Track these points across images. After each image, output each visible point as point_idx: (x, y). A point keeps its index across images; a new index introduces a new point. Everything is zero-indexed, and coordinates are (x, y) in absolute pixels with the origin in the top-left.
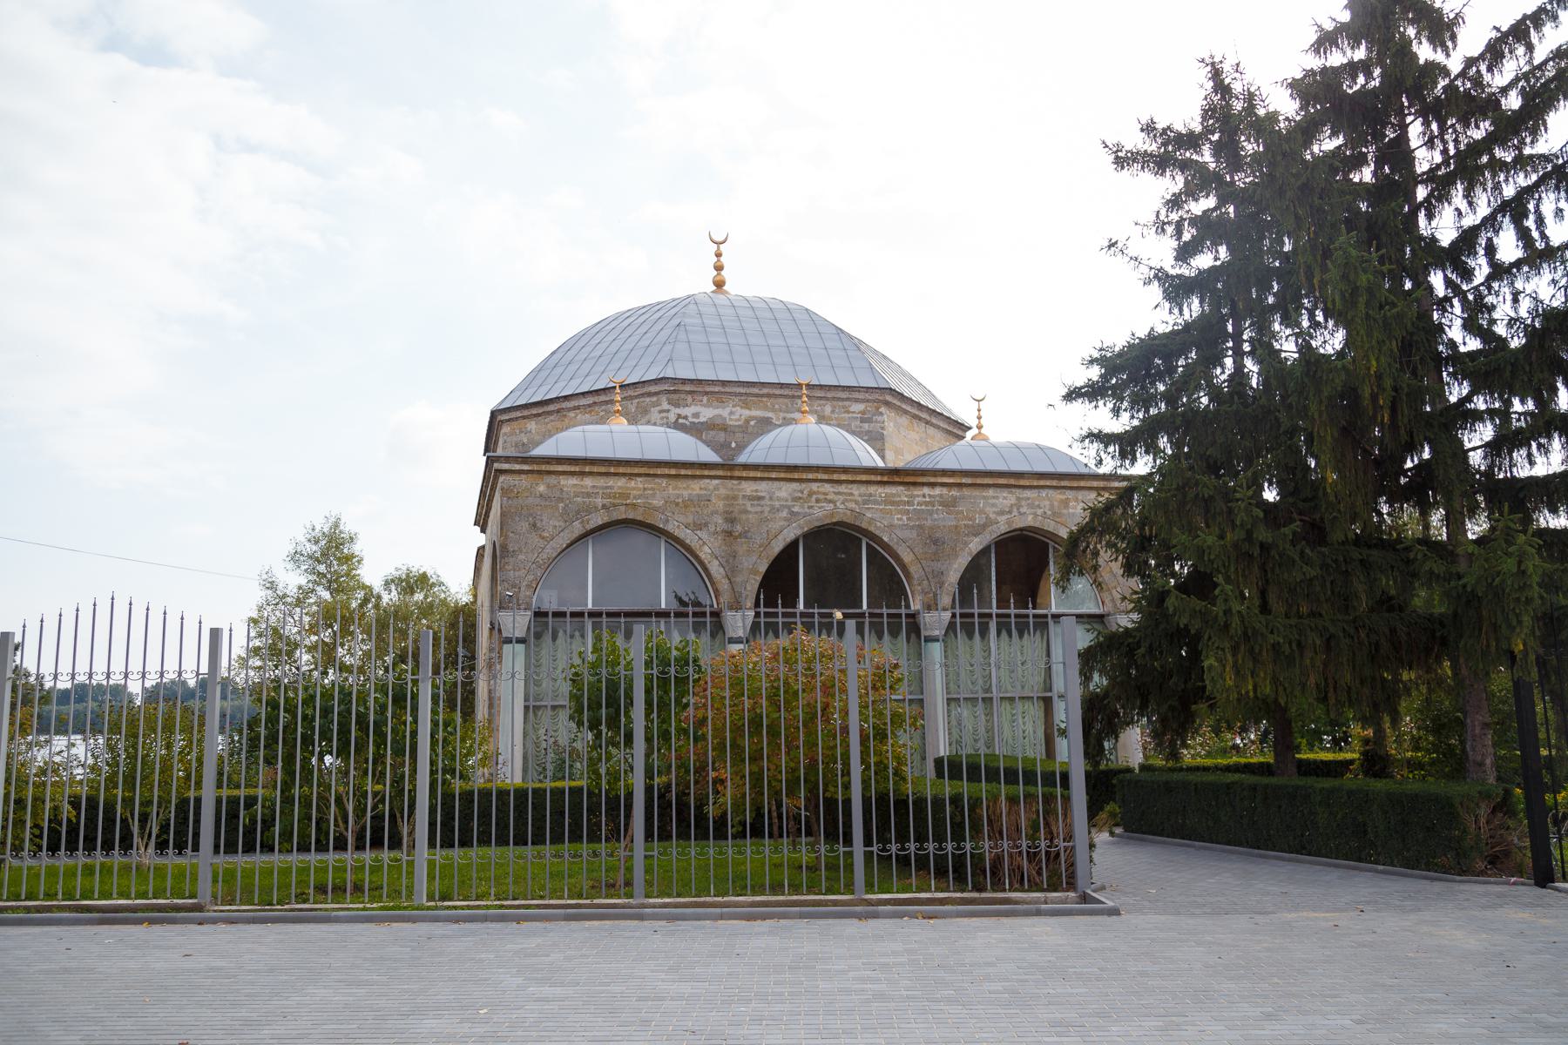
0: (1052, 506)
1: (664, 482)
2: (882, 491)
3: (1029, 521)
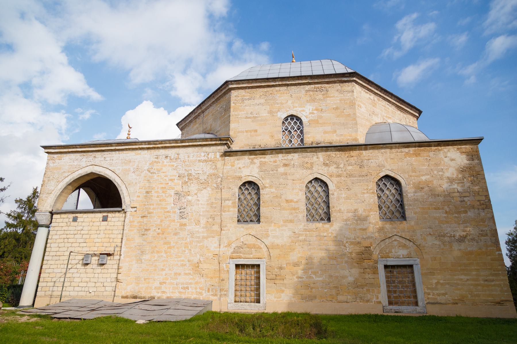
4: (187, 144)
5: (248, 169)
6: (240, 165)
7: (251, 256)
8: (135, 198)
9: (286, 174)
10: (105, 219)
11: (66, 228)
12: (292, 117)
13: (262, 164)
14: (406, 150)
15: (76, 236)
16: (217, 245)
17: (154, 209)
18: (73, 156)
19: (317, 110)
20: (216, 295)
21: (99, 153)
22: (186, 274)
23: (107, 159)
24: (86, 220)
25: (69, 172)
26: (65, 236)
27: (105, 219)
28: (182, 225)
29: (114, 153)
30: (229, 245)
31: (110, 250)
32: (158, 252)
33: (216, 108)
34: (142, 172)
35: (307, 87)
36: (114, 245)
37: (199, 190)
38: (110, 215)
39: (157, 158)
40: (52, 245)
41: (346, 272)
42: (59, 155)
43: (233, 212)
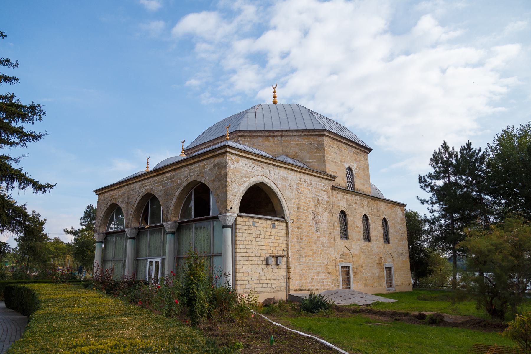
0: (200, 169)
1: (118, 190)
2: (156, 179)
3: (193, 178)
4: (317, 175)
5: (342, 201)
6: (339, 198)
7: (347, 261)
8: (292, 212)
9: (355, 209)
10: (274, 227)
11: (248, 231)
12: (349, 168)
13: (347, 199)
14: (389, 205)
15: (258, 239)
16: (333, 252)
17: (303, 222)
18: (247, 161)
19: (357, 167)
20: (335, 286)
21: (265, 165)
22: (322, 272)
23: (271, 172)
24: (262, 225)
25: (246, 177)
26: (248, 239)
27: (274, 227)
28: (318, 237)
29: (274, 167)
30: (338, 254)
31: (281, 253)
32: (309, 256)
33: (306, 142)
34: (293, 190)
35: (354, 150)
36: (282, 249)
37: (323, 212)
38: (276, 223)
39: (300, 180)
40: (242, 246)
41: (376, 271)
42: (236, 157)
43: (337, 231)
